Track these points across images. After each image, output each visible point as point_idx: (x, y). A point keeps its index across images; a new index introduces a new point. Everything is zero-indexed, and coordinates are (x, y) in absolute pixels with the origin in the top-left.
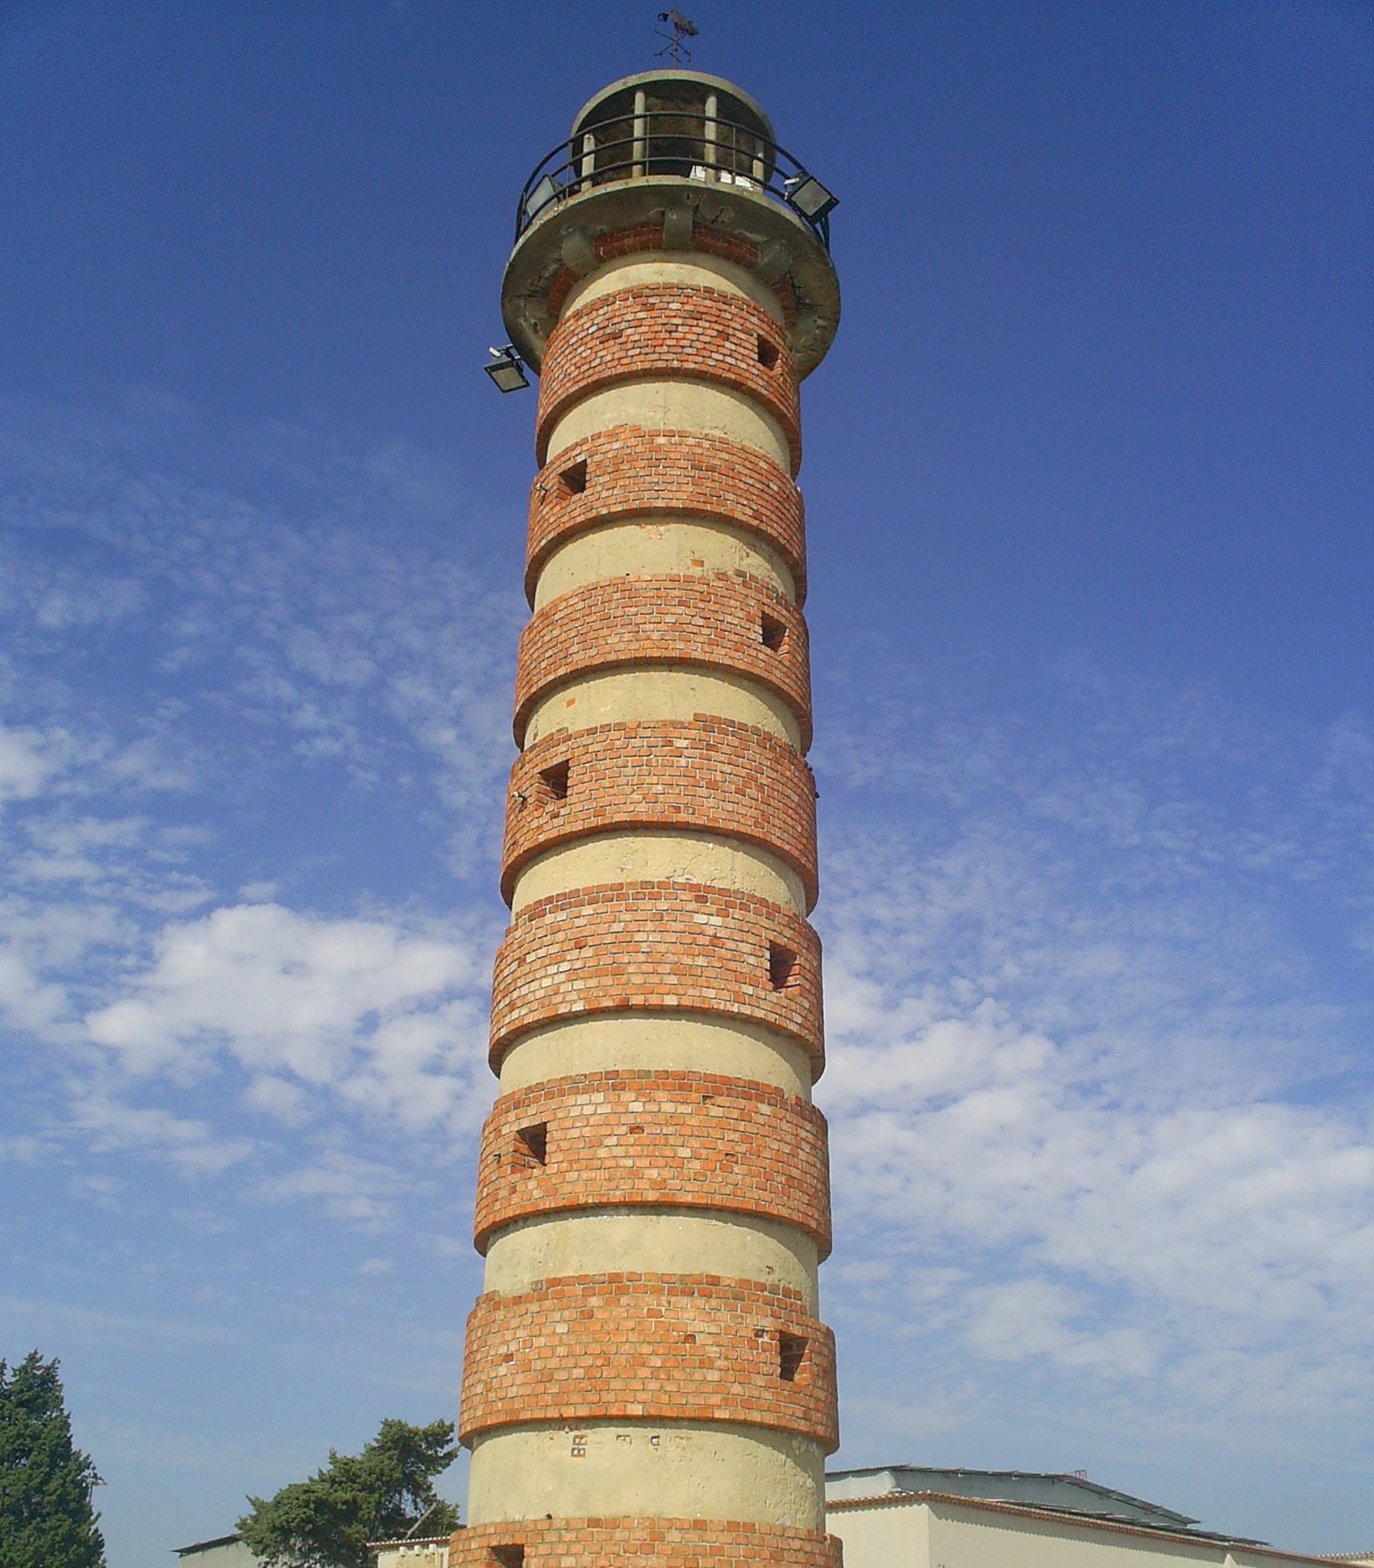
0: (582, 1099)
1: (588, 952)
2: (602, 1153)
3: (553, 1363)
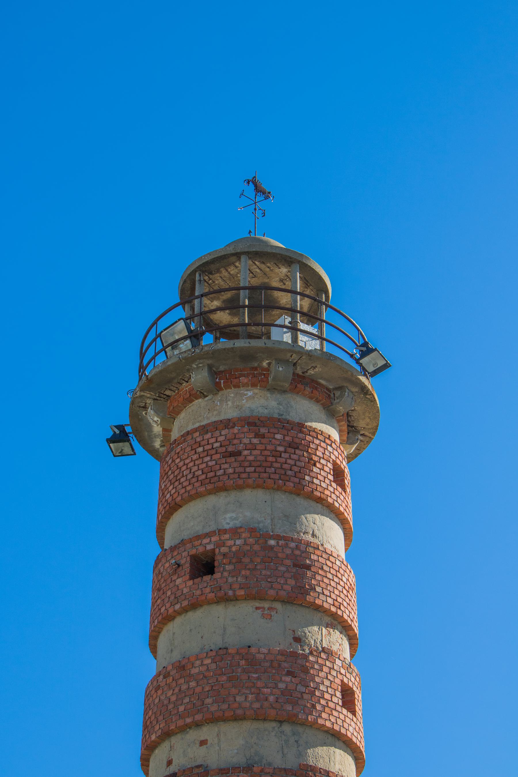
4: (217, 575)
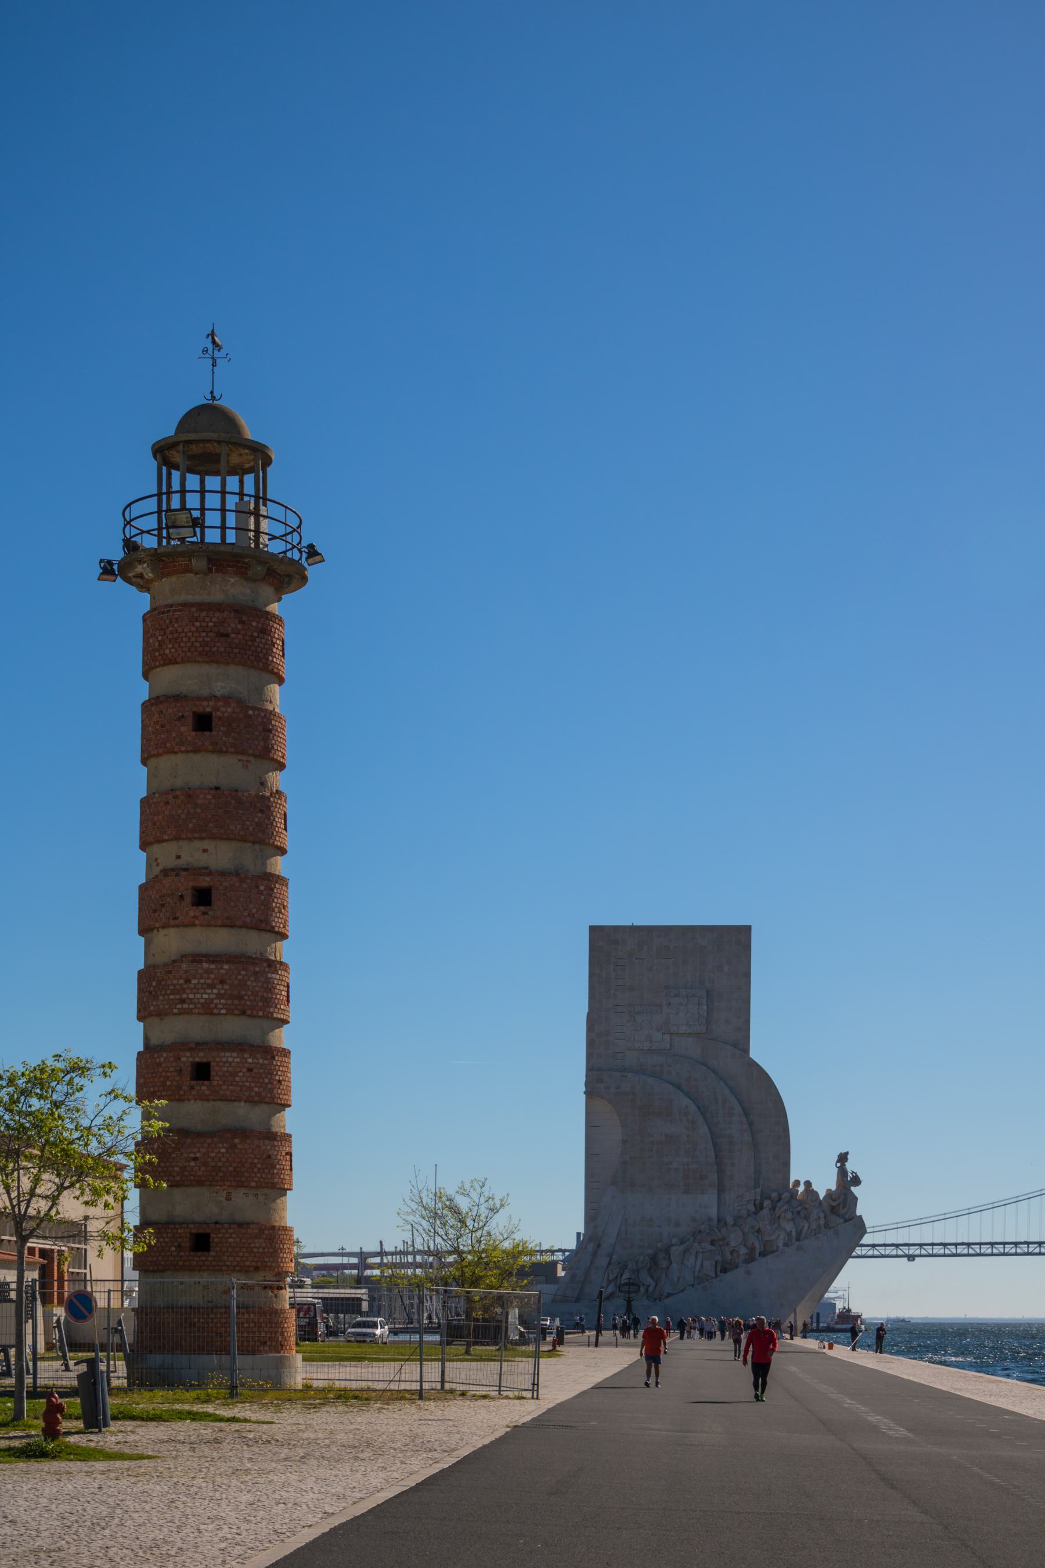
0: (227, 1054)
1: (226, 987)
2: (237, 1079)
3: (219, 1164)
4: (214, 733)
